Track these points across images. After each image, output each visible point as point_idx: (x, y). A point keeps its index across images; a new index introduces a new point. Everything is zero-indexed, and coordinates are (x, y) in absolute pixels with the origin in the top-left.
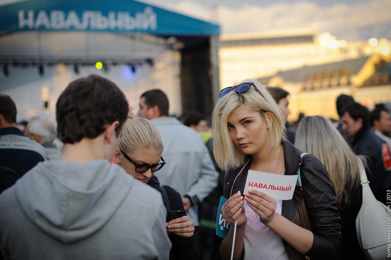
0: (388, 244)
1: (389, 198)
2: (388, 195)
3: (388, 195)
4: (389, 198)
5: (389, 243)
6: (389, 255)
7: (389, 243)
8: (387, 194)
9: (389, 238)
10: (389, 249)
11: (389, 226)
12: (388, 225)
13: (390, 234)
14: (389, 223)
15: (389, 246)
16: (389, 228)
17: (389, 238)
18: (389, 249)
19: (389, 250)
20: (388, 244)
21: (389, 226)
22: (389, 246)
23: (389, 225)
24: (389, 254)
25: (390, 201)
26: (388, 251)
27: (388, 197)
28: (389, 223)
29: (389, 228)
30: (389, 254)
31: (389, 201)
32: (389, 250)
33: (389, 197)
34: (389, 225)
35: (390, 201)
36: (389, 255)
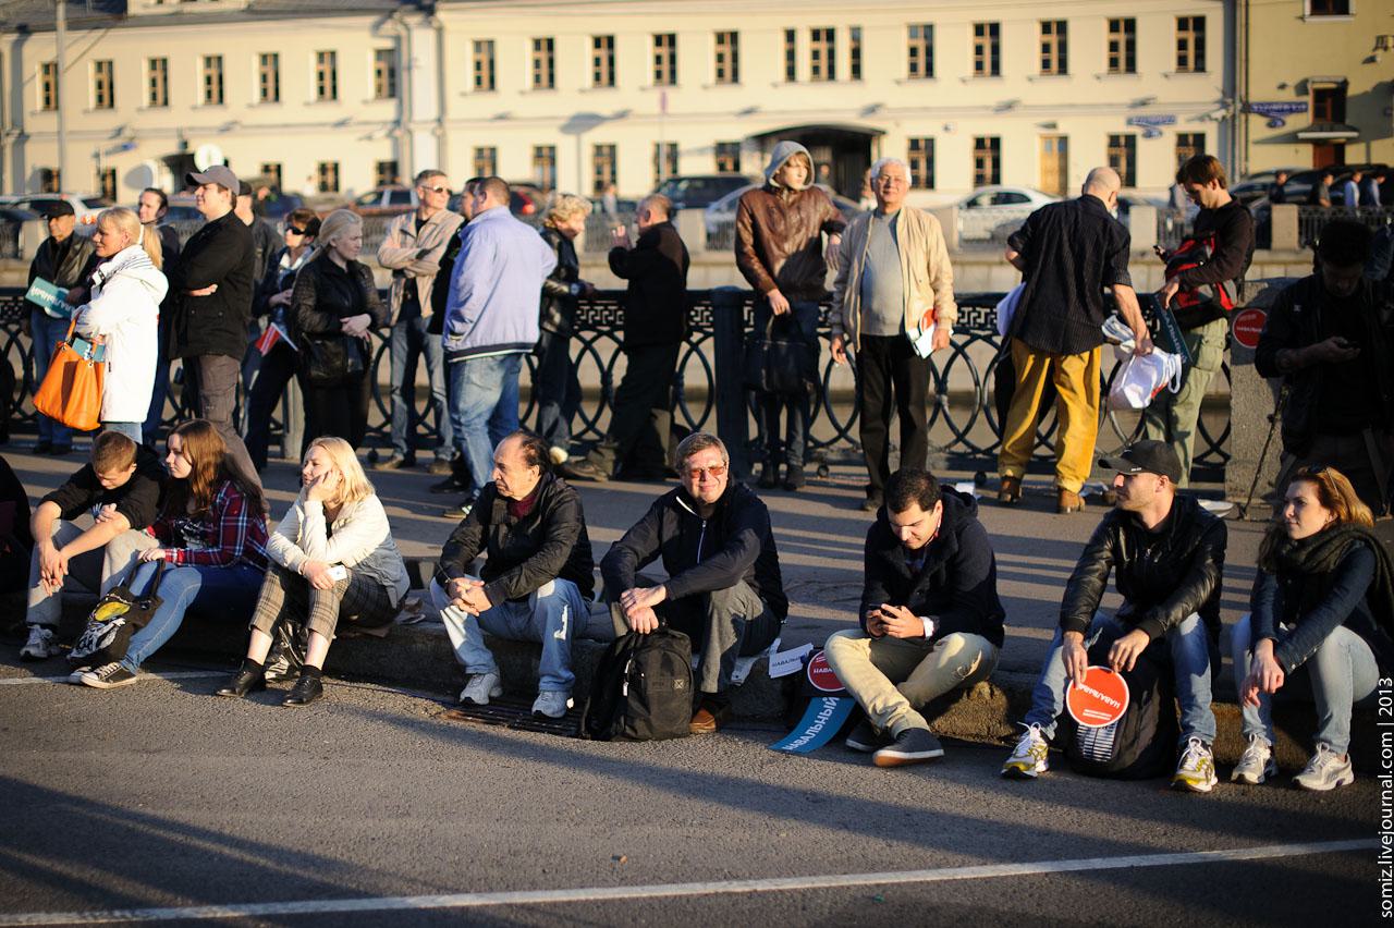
0: (1384, 871)
1: (1388, 708)
2: (1384, 695)
3: (1384, 695)
4: (1388, 708)
5: (1386, 867)
6: (1386, 911)
7: (1386, 867)
8: (1380, 692)
9: (1386, 850)
10: (1386, 887)
11: (1388, 808)
12: (1385, 804)
13: (1389, 836)
14: (1386, 795)
15: (1386, 877)
16: (1388, 814)
17: (1386, 850)
18: (1386, 887)
19: (1386, 893)
20: (1384, 871)
21: (1388, 808)
22: (1386, 877)
23: (1387, 801)
24: (1387, 905)
25: (1390, 719)
26: (1384, 896)
27: (1382, 702)
28: (1386, 795)
29: (1388, 814)
30: (1387, 905)
31: (1385, 717)
32: (1386, 893)
33: (1388, 702)
34: (1387, 801)
35: (1390, 719)
36: (1386, 911)
